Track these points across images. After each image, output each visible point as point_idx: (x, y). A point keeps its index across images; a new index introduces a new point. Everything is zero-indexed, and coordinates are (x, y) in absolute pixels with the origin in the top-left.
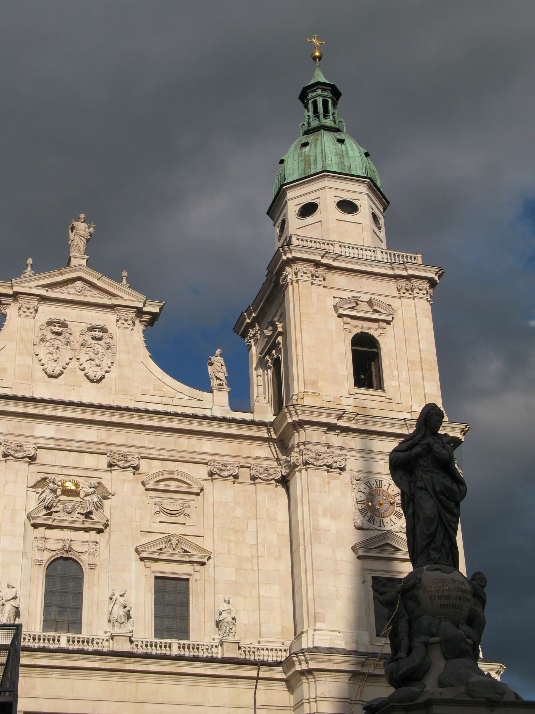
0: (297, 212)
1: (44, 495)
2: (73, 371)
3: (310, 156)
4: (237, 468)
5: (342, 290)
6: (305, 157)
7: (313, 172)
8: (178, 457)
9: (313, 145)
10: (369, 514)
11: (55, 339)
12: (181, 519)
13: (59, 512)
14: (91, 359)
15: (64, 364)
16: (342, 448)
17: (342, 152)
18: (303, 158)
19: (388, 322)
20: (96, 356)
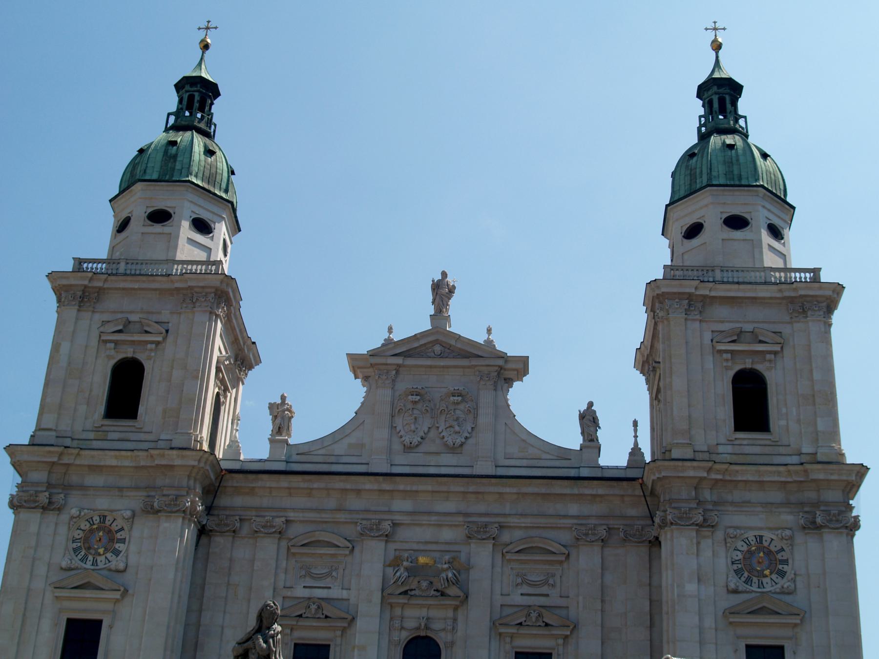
0: (683, 234)
1: (398, 574)
3: (696, 168)
4: (605, 531)
5: (722, 322)
6: (691, 168)
7: (698, 186)
8: (541, 523)
9: (700, 156)
10: (746, 574)
11: (413, 409)
12: (544, 590)
13: (415, 590)
14: (451, 427)
15: (422, 434)
16: (715, 503)
17: (732, 159)
18: (689, 172)
19: (775, 353)
20: (455, 423)
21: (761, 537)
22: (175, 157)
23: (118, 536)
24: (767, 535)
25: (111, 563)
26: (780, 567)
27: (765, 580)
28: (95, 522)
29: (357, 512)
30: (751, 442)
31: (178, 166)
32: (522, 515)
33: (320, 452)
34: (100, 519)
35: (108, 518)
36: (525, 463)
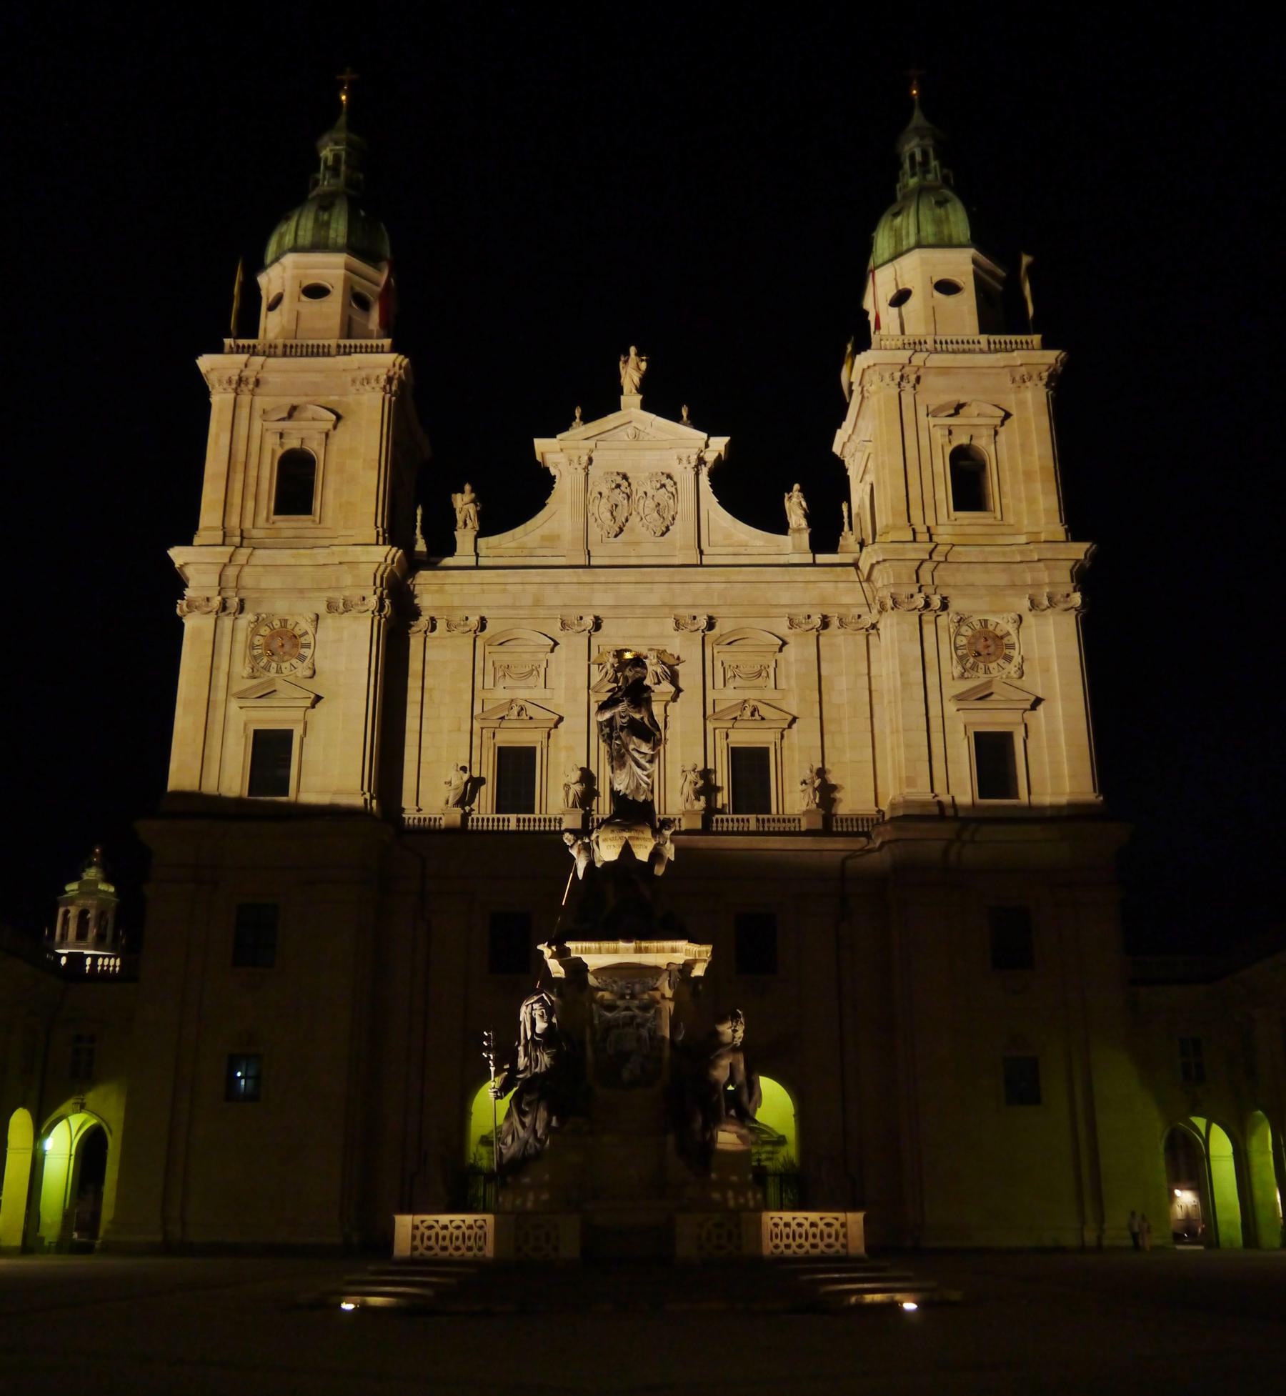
2: (632, 530)
3: (901, 229)
7: (905, 248)
12: (759, 682)
21: (986, 621)
22: (327, 225)
23: (303, 640)
24: (992, 619)
25: (297, 670)
26: (1007, 651)
27: (993, 666)
28: (276, 627)
29: (556, 607)
30: (973, 521)
31: (332, 234)
32: (731, 605)
33: (513, 544)
34: (281, 623)
35: (289, 623)
36: (731, 550)
